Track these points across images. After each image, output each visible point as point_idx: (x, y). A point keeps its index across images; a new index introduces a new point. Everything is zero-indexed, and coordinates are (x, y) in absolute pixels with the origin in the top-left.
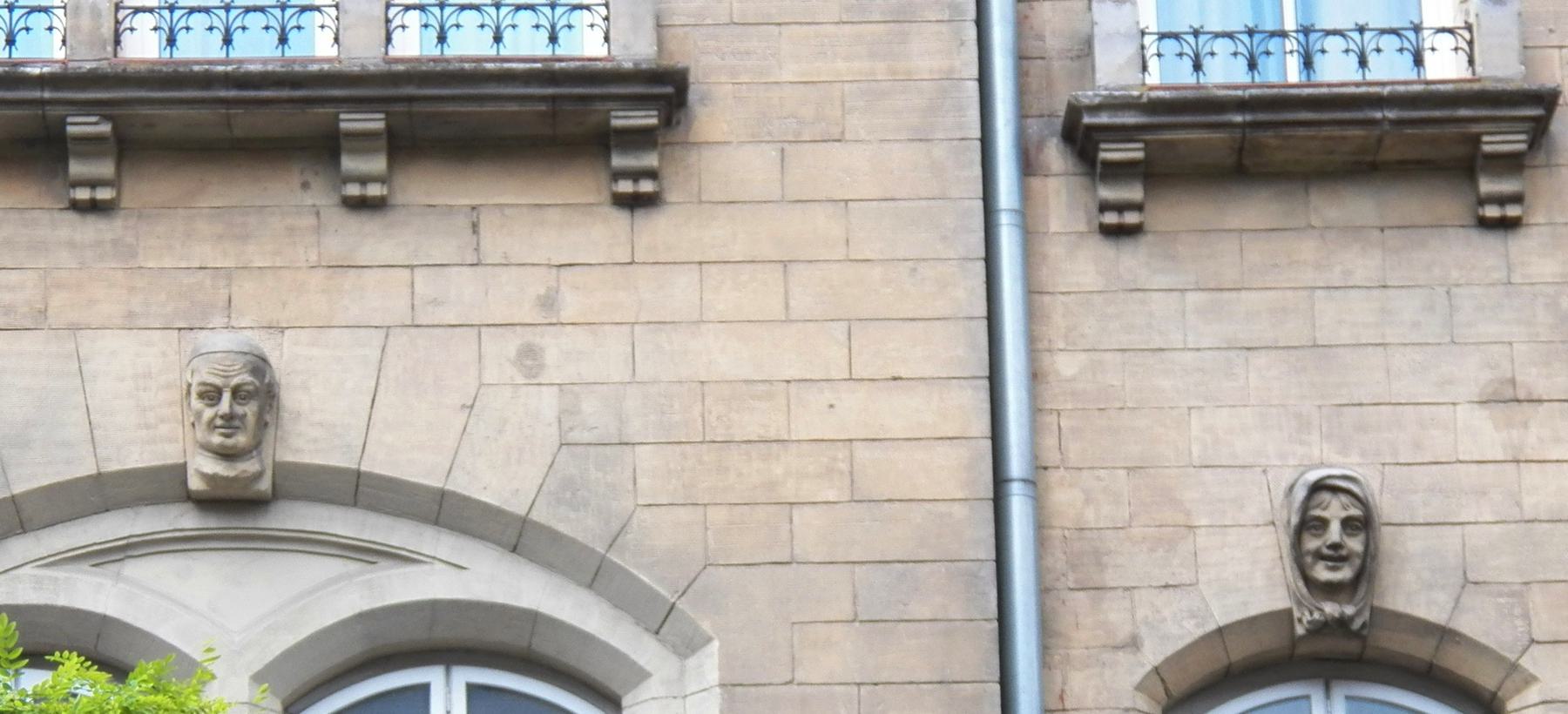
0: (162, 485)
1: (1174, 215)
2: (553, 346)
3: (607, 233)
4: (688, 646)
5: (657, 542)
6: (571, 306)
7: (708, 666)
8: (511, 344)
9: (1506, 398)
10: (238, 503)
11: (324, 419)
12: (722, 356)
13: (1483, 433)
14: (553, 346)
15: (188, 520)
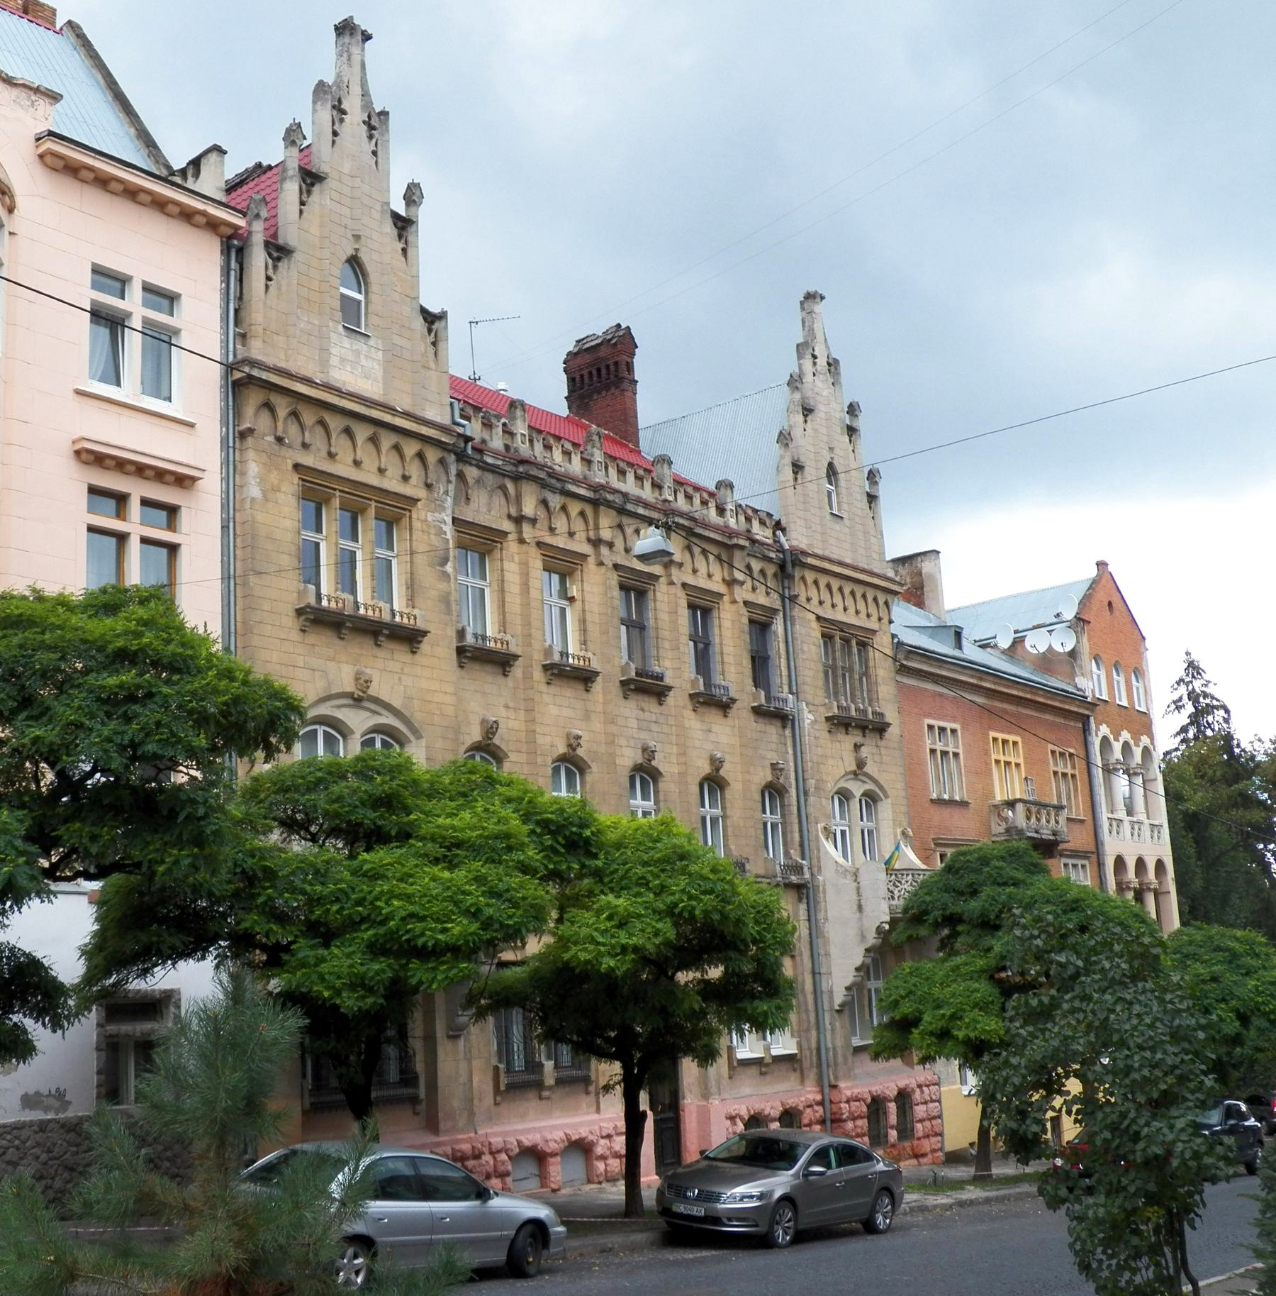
0: (350, 695)
1: (469, 665)
2: (403, 677)
3: (407, 657)
4: (419, 736)
5: (417, 718)
6: (406, 671)
7: (423, 742)
8: (396, 677)
9: (507, 707)
10: (357, 700)
11: (378, 688)
12: (425, 684)
13: (503, 712)
14: (403, 677)
15: (351, 702)
